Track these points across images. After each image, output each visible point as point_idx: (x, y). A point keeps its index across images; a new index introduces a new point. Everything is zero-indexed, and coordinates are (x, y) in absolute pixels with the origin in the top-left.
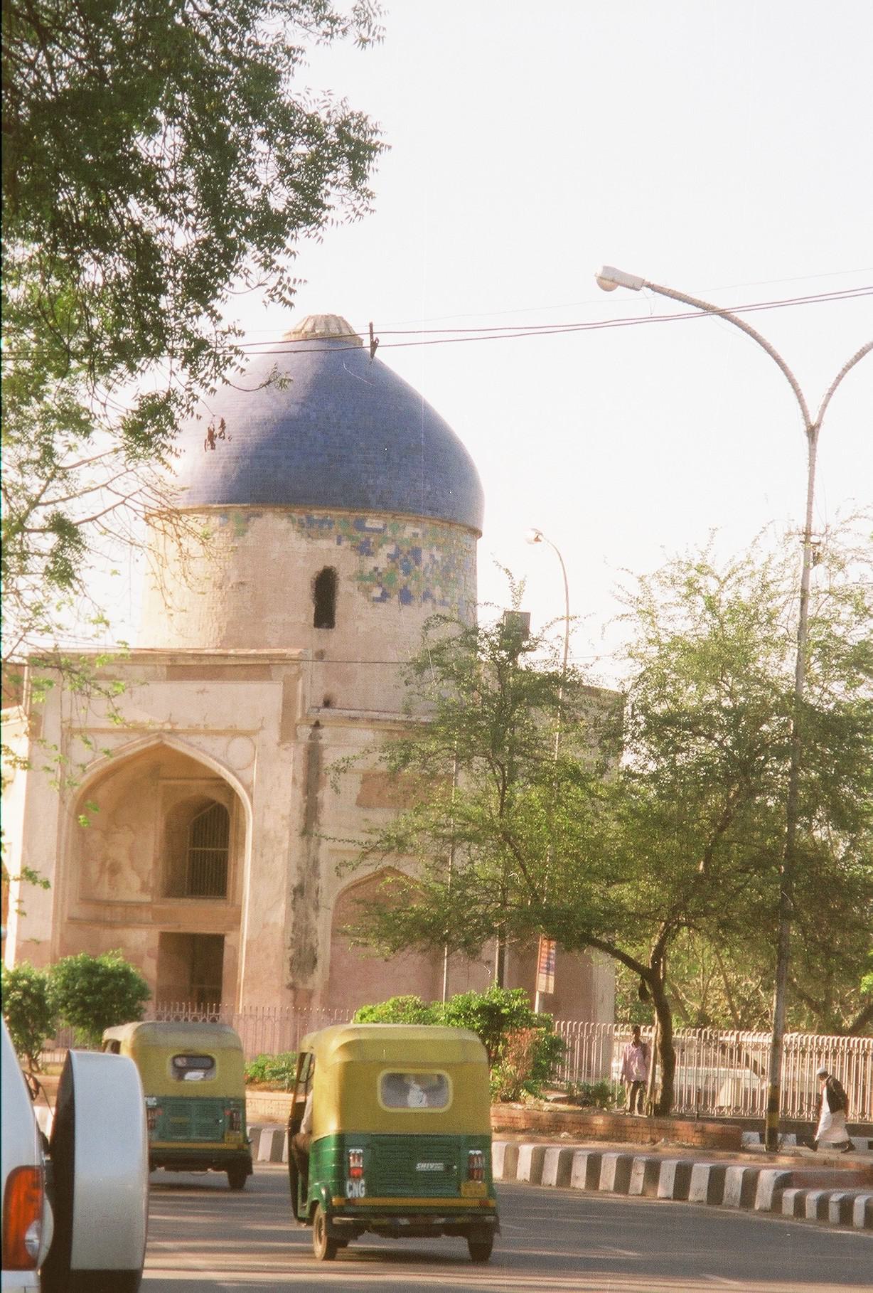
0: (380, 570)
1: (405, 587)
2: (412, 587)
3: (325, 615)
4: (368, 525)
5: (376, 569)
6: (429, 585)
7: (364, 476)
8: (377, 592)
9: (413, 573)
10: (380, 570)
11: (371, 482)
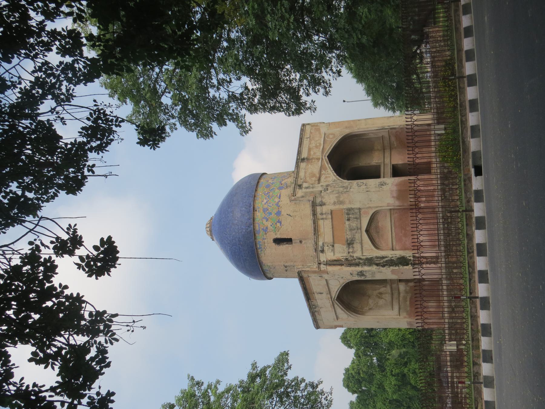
2: (275, 211)
3: (289, 241)
5: (271, 226)
6: (274, 204)
7: (243, 233)
8: (278, 224)
9: (271, 211)
11: (244, 231)
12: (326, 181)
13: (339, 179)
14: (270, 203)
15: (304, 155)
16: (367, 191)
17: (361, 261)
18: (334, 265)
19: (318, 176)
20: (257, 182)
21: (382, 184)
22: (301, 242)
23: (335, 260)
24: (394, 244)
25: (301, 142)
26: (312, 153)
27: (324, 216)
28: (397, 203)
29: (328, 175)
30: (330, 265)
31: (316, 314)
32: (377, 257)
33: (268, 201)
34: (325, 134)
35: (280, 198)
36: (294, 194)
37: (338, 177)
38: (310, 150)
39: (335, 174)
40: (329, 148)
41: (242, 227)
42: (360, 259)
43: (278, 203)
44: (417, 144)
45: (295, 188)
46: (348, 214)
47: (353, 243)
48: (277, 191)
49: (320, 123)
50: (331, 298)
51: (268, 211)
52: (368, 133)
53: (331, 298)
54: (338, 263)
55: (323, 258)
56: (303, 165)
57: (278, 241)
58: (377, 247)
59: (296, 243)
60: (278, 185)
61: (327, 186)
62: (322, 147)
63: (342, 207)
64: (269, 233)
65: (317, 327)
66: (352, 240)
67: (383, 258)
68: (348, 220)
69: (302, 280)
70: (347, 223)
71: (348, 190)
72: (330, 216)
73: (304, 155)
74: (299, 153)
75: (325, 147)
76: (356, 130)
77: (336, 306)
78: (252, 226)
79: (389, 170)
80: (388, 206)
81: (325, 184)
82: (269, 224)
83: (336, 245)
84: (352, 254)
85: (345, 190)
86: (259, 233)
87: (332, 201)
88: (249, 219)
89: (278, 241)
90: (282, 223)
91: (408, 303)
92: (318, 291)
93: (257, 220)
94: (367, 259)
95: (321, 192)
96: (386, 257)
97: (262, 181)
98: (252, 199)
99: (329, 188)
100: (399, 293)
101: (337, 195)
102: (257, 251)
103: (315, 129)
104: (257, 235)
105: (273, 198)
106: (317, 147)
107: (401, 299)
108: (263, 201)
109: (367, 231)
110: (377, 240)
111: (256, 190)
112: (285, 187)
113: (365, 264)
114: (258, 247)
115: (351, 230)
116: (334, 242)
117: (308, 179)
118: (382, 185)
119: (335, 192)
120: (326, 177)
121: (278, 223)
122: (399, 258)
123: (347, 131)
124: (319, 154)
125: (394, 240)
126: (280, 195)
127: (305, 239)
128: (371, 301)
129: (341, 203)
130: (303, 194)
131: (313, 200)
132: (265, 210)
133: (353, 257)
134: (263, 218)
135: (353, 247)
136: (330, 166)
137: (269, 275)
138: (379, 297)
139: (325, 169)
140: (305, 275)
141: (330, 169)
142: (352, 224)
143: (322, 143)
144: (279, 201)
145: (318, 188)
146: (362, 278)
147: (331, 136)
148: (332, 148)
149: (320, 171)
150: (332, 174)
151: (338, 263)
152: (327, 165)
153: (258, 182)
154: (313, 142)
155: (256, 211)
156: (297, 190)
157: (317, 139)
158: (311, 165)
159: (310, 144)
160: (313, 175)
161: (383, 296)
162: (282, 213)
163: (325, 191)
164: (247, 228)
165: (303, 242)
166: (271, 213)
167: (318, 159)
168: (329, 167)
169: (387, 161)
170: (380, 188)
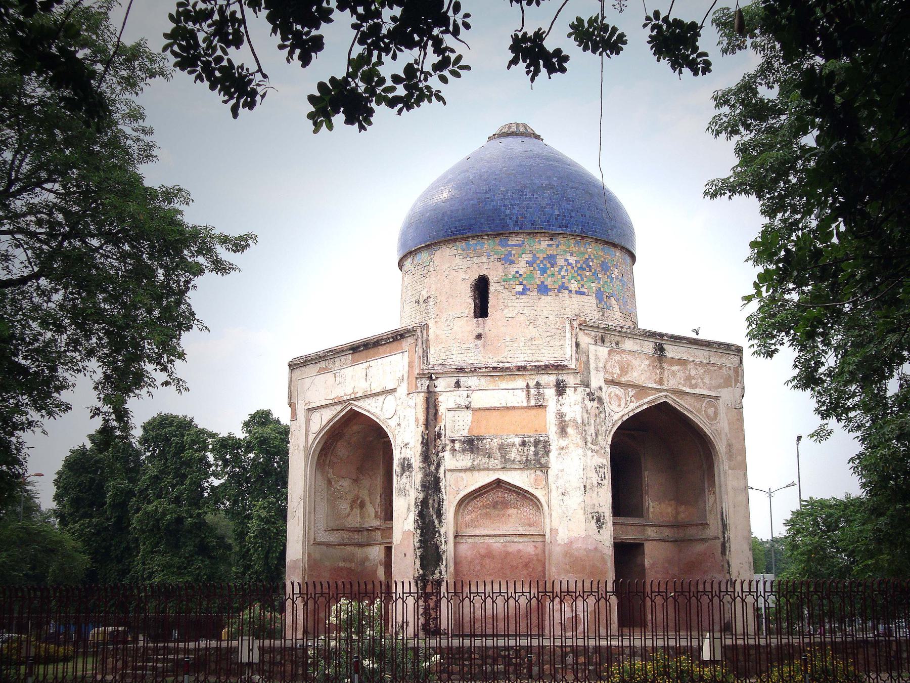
0: (520, 273)
1: (543, 282)
2: (549, 282)
3: (481, 310)
4: (509, 243)
5: (517, 272)
6: (564, 280)
8: (519, 288)
9: (549, 273)
10: (520, 273)
11: (508, 212)
12: (610, 397)
13: (613, 425)
14: (567, 271)
15: (672, 351)
16: (585, 487)
17: (433, 468)
18: (427, 409)
19: (623, 380)
20: (616, 241)
21: (599, 520)
22: (479, 337)
23: (436, 411)
24: (469, 540)
25: (702, 345)
26: (676, 368)
27: (533, 391)
28: (557, 551)
29: (623, 401)
30: (427, 400)
31: (323, 365)
32: (440, 502)
33: (572, 268)
34: (717, 398)
35: (578, 293)
36: (583, 326)
37: (620, 423)
38: (682, 362)
39: (625, 419)
40: (684, 405)
41: (517, 208)
42: (438, 466)
43: (567, 288)
44: (602, 602)
45: (599, 328)
46: (536, 443)
47: (472, 452)
48: (594, 286)
49: (743, 389)
50: (355, 399)
51: (549, 266)
52: (714, 493)
53: (355, 399)
54: (431, 417)
55: (442, 384)
56: (649, 347)
57: (481, 288)
58: (465, 502)
59: (478, 326)
60: (608, 290)
61: (600, 400)
62: (688, 390)
63: (552, 430)
64: (501, 268)
65: (294, 366)
66: (478, 448)
67: (439, 515)
68: (524, 444)
69: (398, 336)
70: (517, 441)
71: (589, 444)
72: (532, 403)
73: (672, 351)
74: (676, 339)
75: (687, 397)
76: (723, 466)
77: (339, 408)
78: (517, 229)
79: (631, 535)
80: (551, 530)
81: (604, 395)
82: (521, 266)
83: (469, 414)
84: (448, 448)
85: (589, 439)
86: (503, 246)
87: (564, 410)
88: (533, 223)
89: (481, 288)
90: (521, 297)
91: (341, 564)
92: (371, 372)
93: (527, 240)
94: (437, 481)
95: (588, 386)
96: (440, 522)
97: (618, 253)
98: (577, 229)
99: (595, 404)
100: (361, 545)
101: (580, 421)
102: (462, 239)
103: (730, 376)
104: (497, 240)
105: (579, 278)
106: (689, 378)
107: (349, 549)
108: (572, 255)
109: (498, 483)
110: (478, 503)
111: (596, 240)
112: (601, 306)
113: (426, 475)
114: (472, 242)
115: (502, 447)
116: (476, 410)
117: (617, 358)
118: (598, 520)
119: (586, 416)
120: (619, 398)
121: (522, 287)
122: (437, 547)
123: (721, 447)
124: (672, 383)
125: (477, 539)
126: (584, 293)
127: (484, 346)
128: (346, 483)
129: (563, 430)
130: (583, 345)
131: (571, 367)
132: (551, 259)
133: (443, 450)
134: (534, 255)
135: (464, 451)
136: (645, 407)
137: (408, 263)
138: (354, 502)
139: (637, 397)
140: (407, 343)
141: (638, 407)
142: (514, 450)
143: (697, 391)
144: (570, 292)
145: (596, 380)
146: (396, 468)
147: (711, 411)
148: (686, 413)
149: (634, 386)
150: (626, 410)
151: (431, 417)
152: (647, 400)
153: (614, 245)
154: (701, 371)
155: (551, 240)
156: (593, 333)
157: (707, 380)
158: (648, 366)
159: (696, 364)
160: (624, 370)
161: (357, 511)
162: (543, 297)
163: (588, 394)
164: (514, 218)
165: (478, 342)
166: (544, 272)
167: (661, 381)
168: (641, 405)
169: (651, 532)
170: (590, 516)
